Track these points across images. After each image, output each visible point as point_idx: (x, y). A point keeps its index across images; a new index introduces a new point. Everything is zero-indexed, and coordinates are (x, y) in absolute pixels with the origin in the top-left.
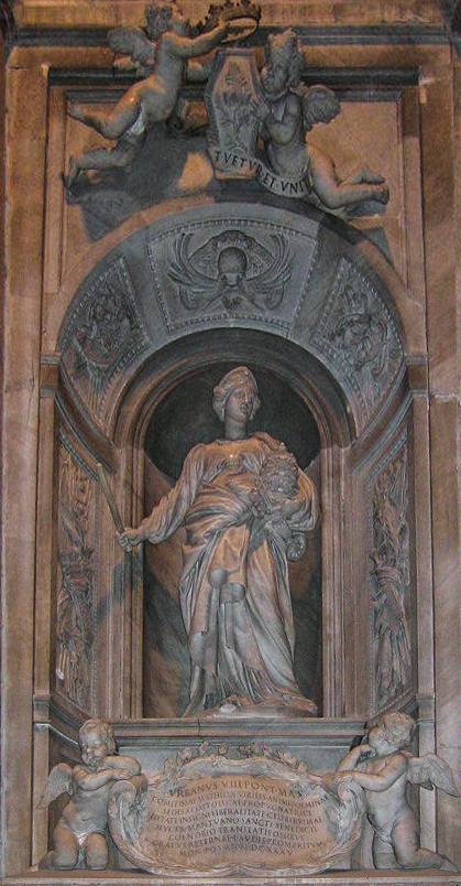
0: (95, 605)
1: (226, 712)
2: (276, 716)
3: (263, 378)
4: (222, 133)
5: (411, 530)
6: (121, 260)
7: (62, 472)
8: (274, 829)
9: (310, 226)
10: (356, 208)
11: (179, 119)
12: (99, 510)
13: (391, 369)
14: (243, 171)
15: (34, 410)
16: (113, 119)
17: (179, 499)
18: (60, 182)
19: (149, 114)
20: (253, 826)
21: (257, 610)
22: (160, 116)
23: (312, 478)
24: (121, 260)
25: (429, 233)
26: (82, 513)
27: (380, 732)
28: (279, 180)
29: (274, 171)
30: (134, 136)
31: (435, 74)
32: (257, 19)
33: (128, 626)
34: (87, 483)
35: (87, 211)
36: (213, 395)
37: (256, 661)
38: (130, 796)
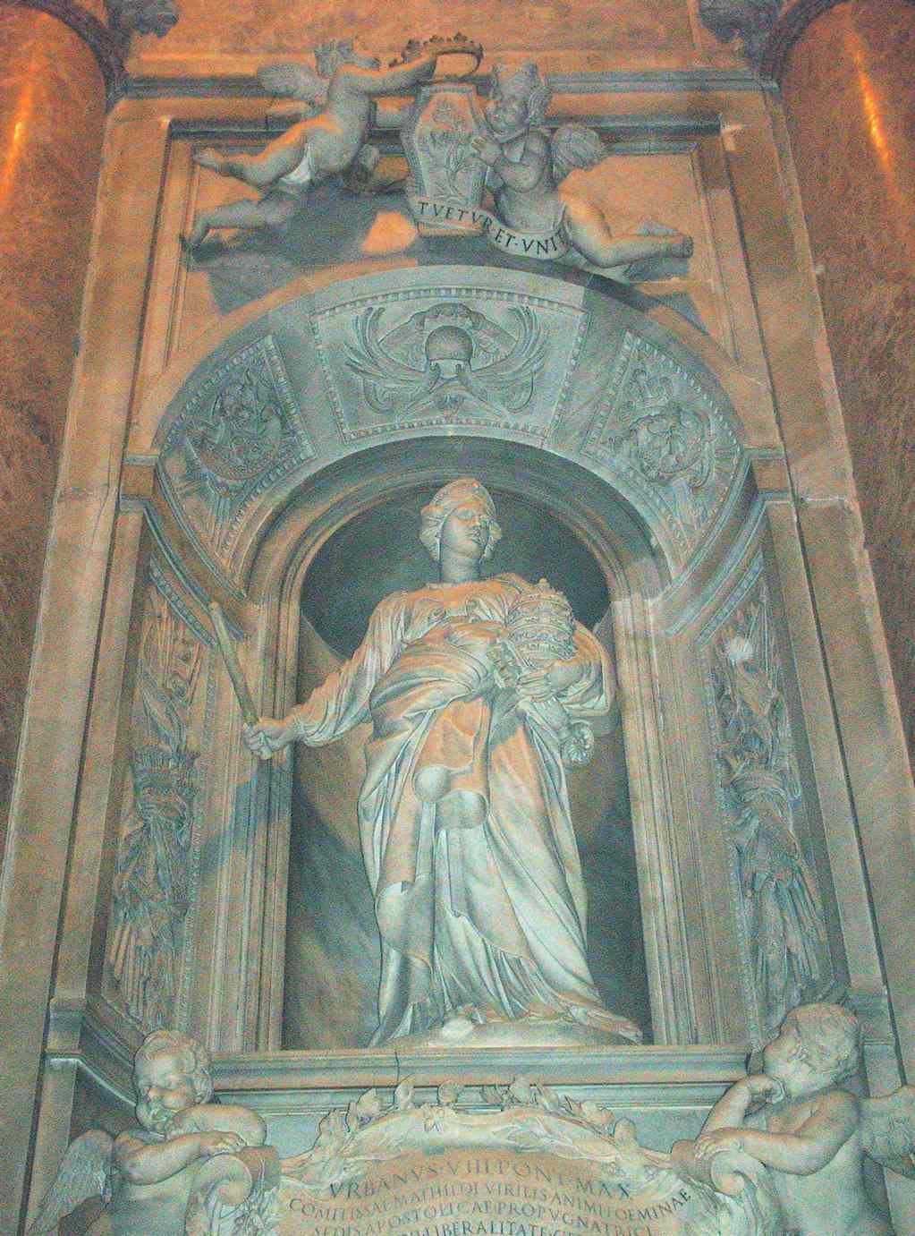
0: (197, 844)
1: (456, 1032)
2: (558, 1042)
3: (504, 502)
4: (428, 182)
5: (791, 701)
6: (269, 340)
7: (147, 623)
9: (574, 293)
10: (643, 267)
11: (363, 168)
12: (215, 693)
13: (722, 475)
14: (462, 226)
15: (104, 527)
16: (264, 164)
17: (361, 673)
18: (176, 245)
19: (317, 160)
21: (509, 842)
22: (336, 162)
23: (604, 645)
24: (269, 340)
26: (181, 693)
27: (789, 1045)
28: (519, 237)
30: (295, 186)
31: (743, 121)
32: (478, 55)
33: (258, 889)
34: (194, 650)
35: (215, 277)
36: (420, 517)
37: (512, 936)
38: (236, 1190)
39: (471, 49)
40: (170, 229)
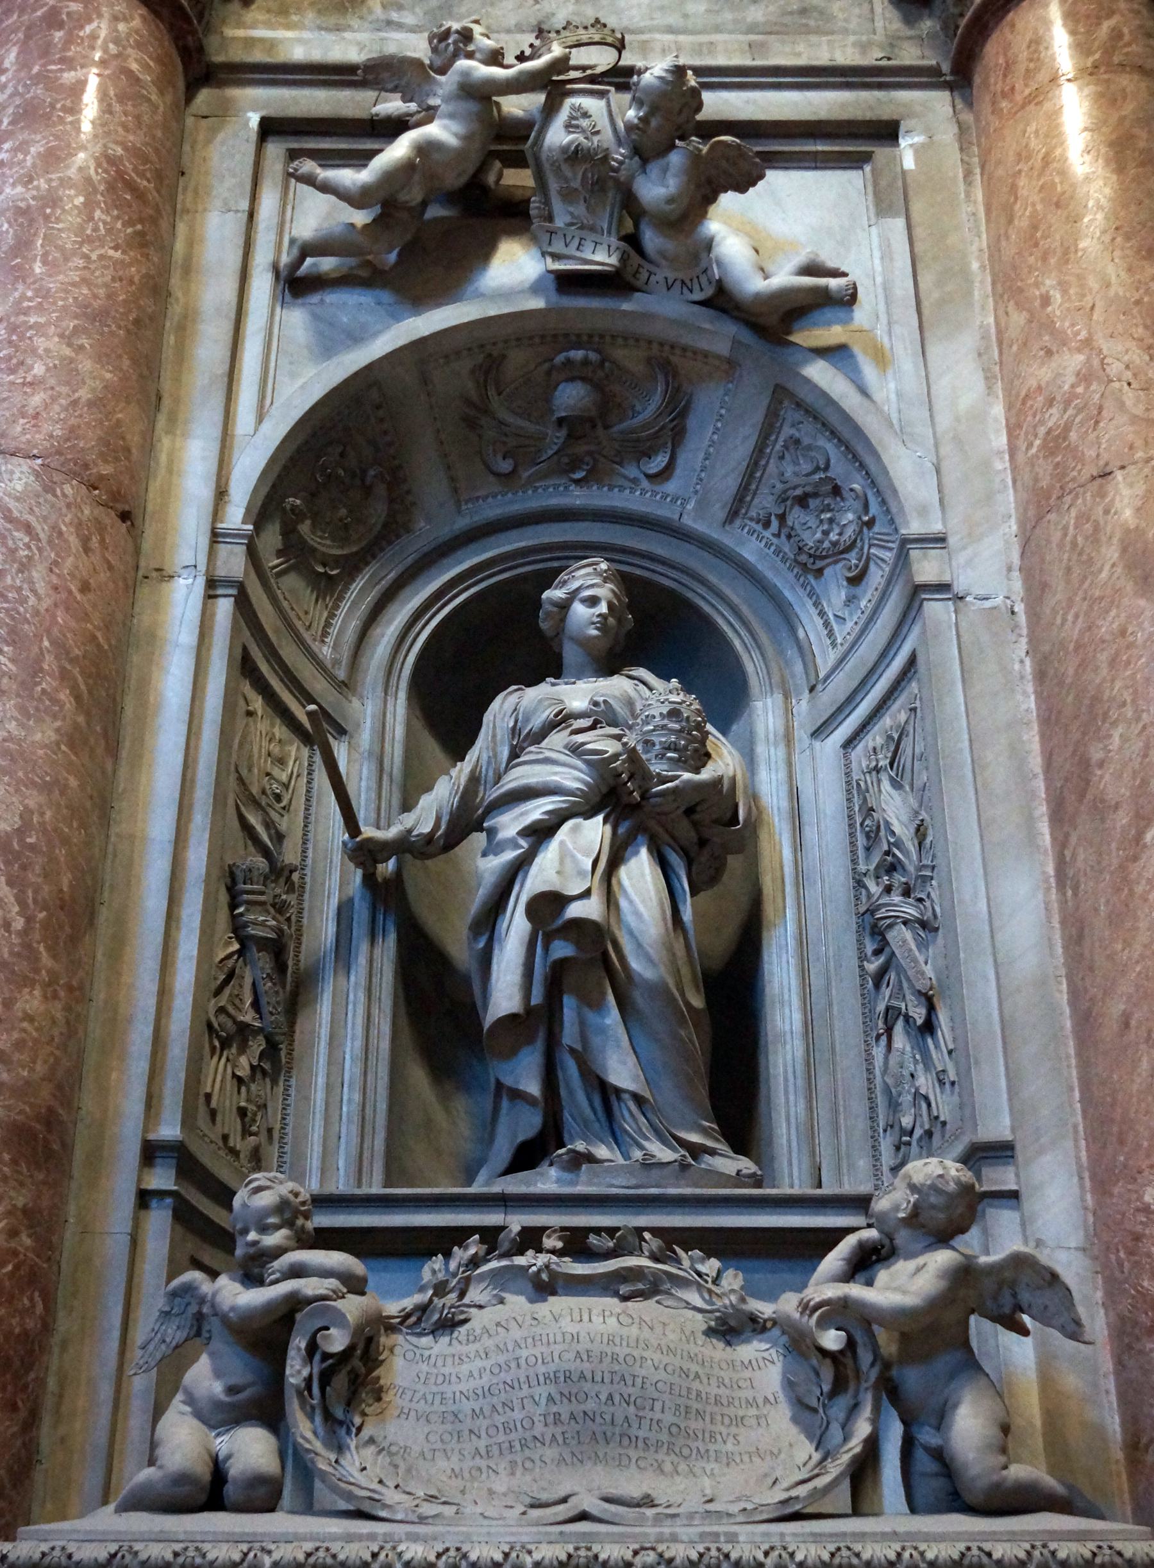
8: (668, 1418)
20: (620, 1411)
25: (933, 351)
26: (278, 797)
29: (650, 262)
32: (620, 46)
35: (316, 317)
39: (610, 40)
40: (262, 257)
